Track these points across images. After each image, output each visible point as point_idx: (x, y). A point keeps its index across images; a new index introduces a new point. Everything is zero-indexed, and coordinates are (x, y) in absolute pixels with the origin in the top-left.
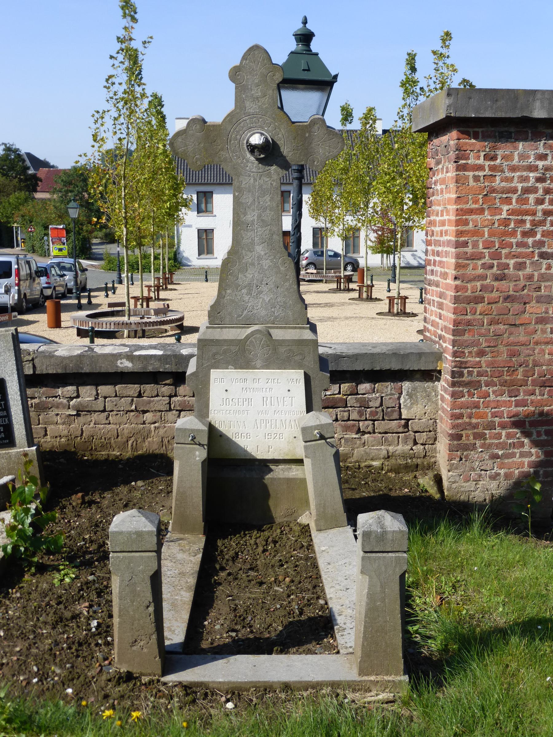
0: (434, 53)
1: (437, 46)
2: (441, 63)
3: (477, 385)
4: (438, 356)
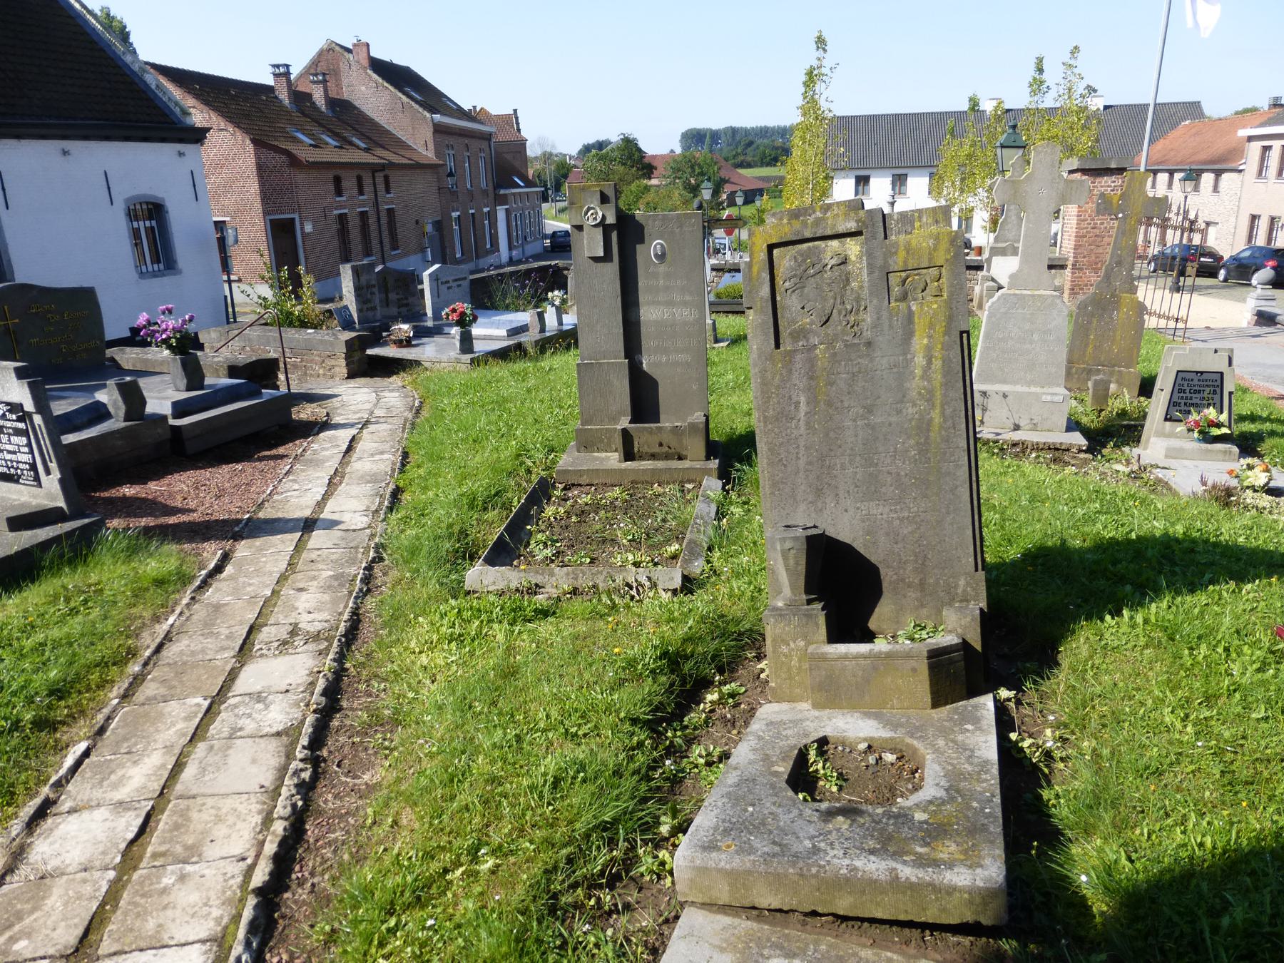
0: (1064, 64)
1: (1066, 57)
2: (1069, 73)
3: (1082, 269)
4: (1067, 259)
